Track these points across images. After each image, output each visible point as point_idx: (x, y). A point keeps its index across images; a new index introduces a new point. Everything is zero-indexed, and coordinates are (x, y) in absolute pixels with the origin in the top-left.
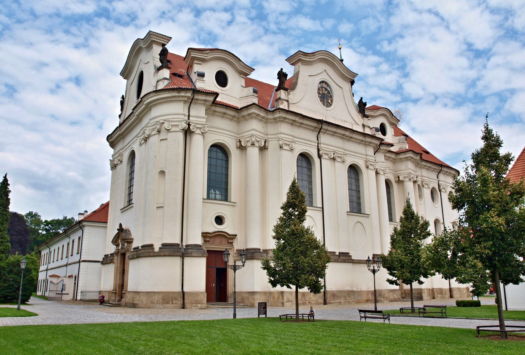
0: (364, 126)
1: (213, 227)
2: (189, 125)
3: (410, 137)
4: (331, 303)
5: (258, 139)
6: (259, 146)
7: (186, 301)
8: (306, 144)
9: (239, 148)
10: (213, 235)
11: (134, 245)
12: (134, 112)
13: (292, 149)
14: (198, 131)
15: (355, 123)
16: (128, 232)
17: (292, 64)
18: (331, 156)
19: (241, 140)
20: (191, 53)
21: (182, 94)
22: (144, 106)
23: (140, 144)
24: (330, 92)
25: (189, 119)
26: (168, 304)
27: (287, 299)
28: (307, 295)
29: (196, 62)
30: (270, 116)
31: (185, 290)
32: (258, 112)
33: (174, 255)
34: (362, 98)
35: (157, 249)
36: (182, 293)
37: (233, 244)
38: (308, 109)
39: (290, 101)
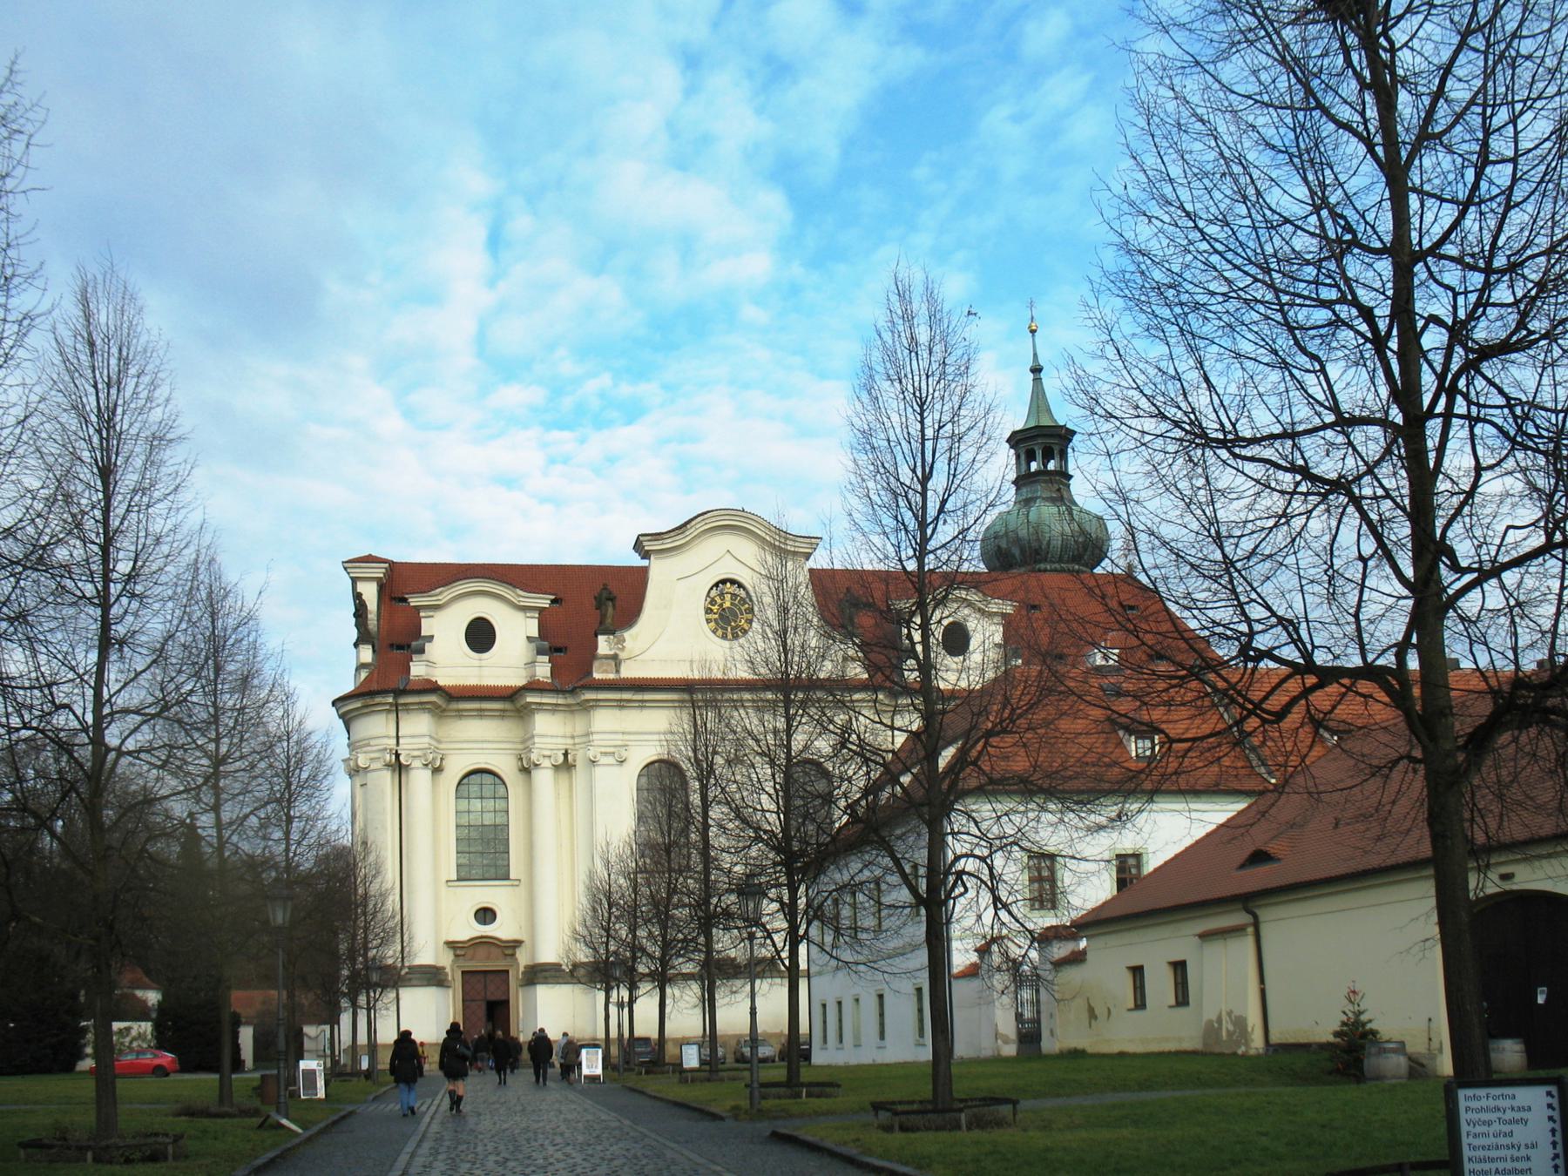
1: (469, 929)
2: (397, 755)
37: (518, 955)
39: (622, 655)
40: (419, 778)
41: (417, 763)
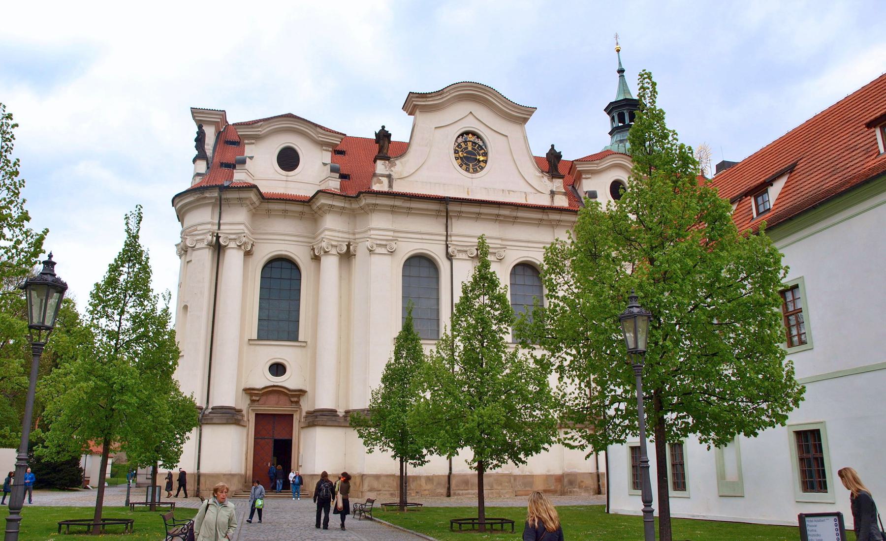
1: (263, 379)
2: (218, 237)
4: (459, 494)
5: (334, 243)
6: (338, 253)
7: (202, 487)
8: (422, 239)
10: (263, 392)
14: (232, 245)
15: (535, 192)
17: (410, 114)
18: (472, 254)
20: (238, 130)
21: (207, 195)
24: (484, 147)
25: (219, 229)
27: (369, 486)
28: (413, 481)
29: (246, 141)
30: (355, 206)
31: (203, 470)
32: (330, 202)
34: (553, 146)
38: (430, 183)
39: (395, 176)
40: (233, 258)
41: (232, 245)
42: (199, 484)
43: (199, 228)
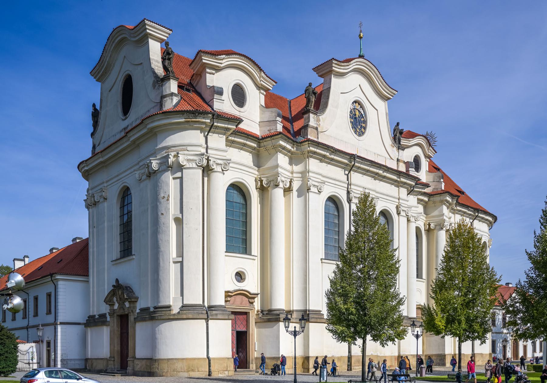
0: (398, 160)
1: (233, 285)
3: (442, 171)
6: (284, 187)
9: (259, 188)
11: (140, 305)
12: (129, 136)
13: (320, 192)
14: (219, 169)
16: (128, 289)
19: (262, 179)
22: (144, 131)
23: (140, 180)
26: (193, 371)
33: (198, 317)
35: (175, 310)
36: (207, 360)
42: (209, 366)
43: (189, 148)
